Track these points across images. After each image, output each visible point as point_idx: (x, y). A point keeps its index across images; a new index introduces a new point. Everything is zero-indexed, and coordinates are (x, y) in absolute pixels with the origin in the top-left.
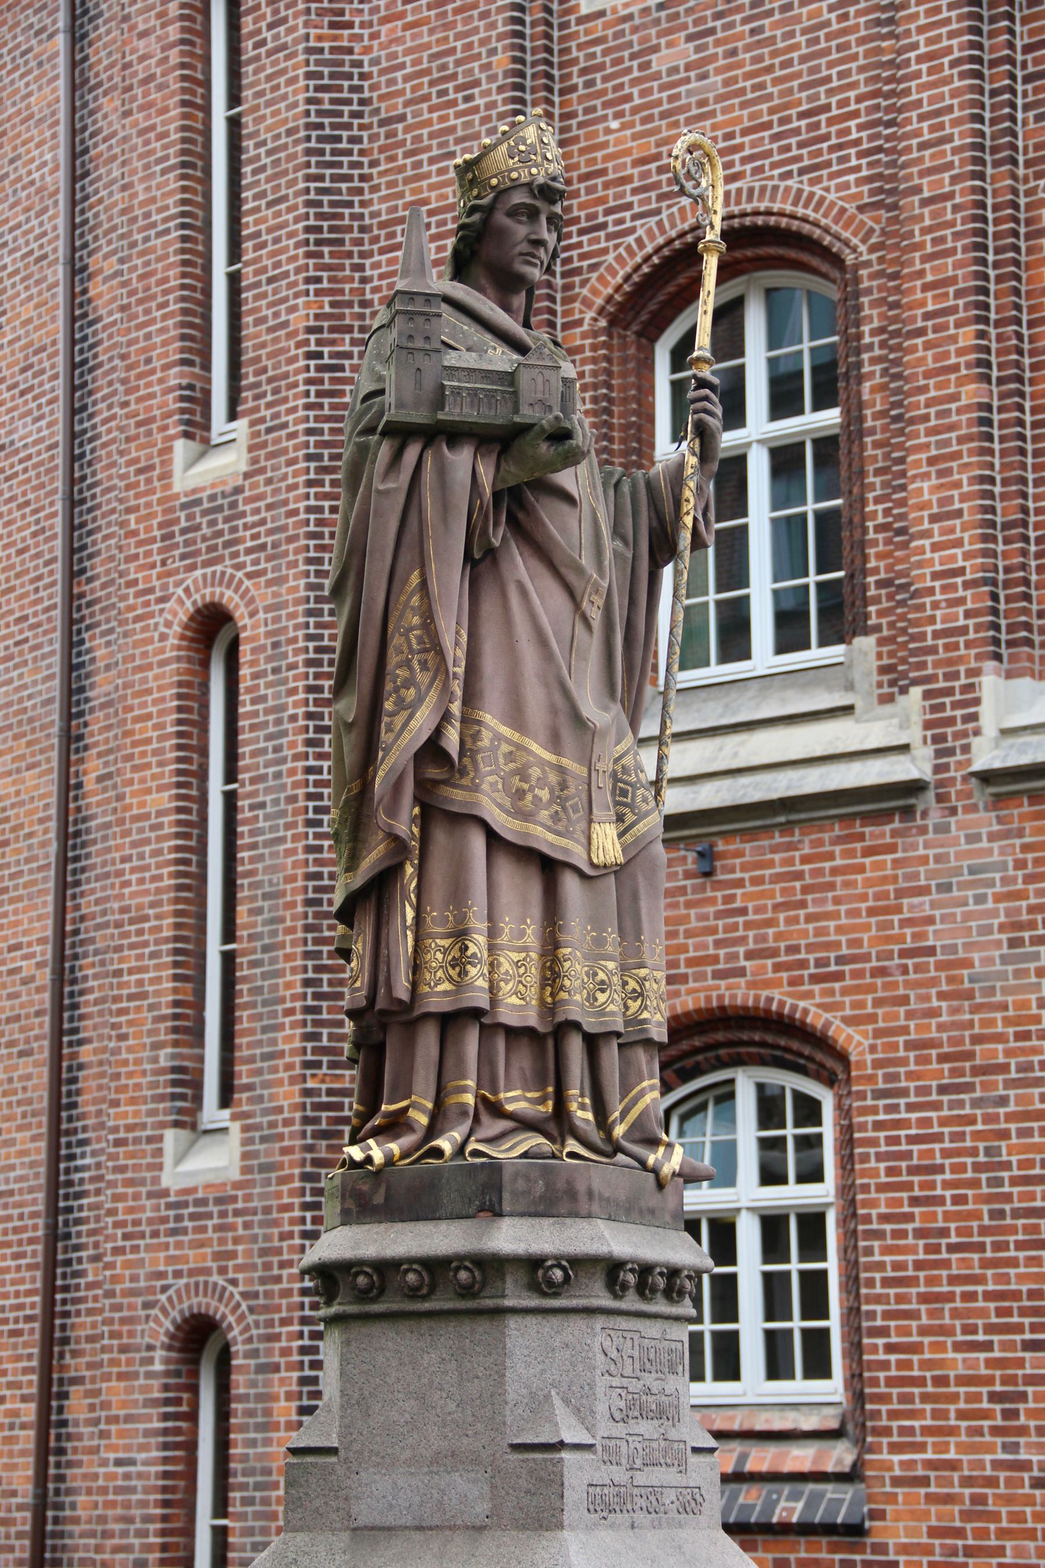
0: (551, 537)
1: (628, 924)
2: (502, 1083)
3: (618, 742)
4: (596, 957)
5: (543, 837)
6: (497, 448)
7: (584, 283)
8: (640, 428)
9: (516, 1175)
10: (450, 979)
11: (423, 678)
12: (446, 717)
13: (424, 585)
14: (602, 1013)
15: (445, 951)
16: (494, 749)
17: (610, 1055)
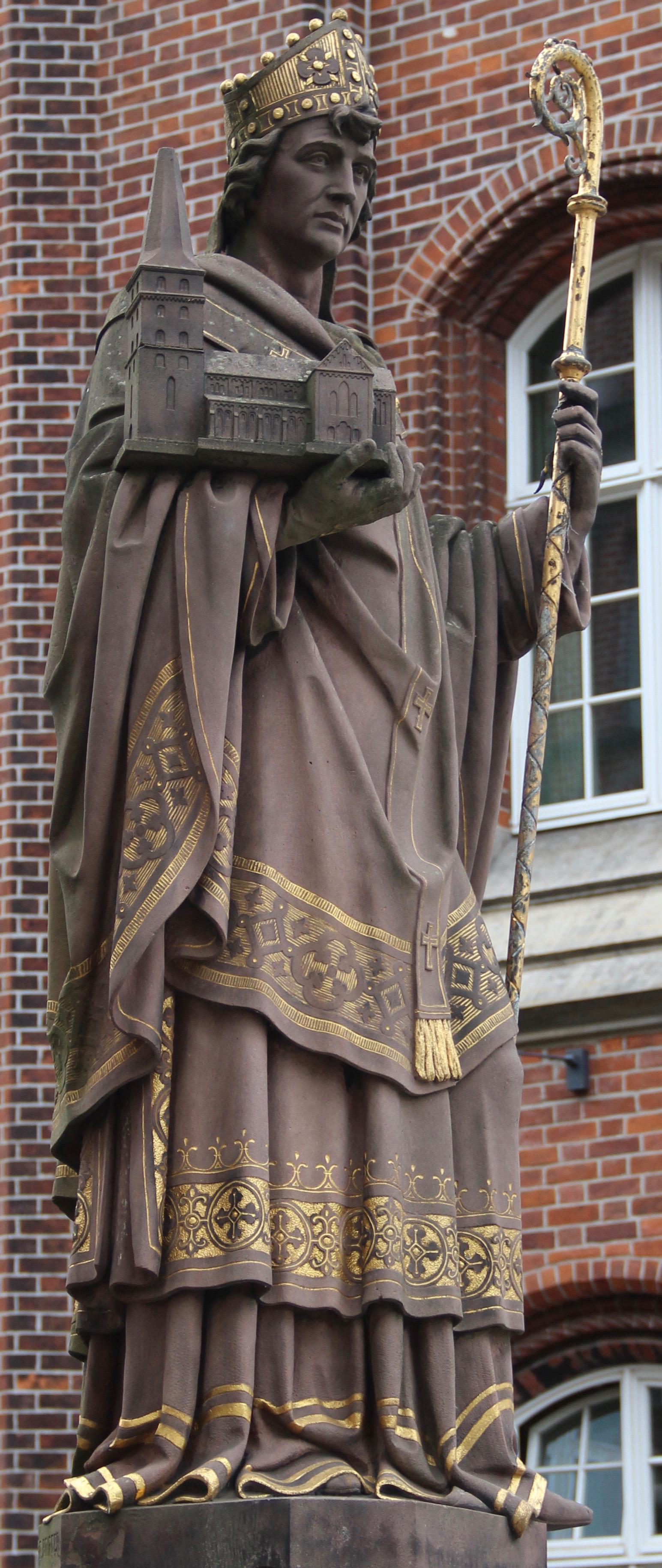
0: (358, 616)
1: (468, 1162)
2: (289, 1388)
3: (454, 906)
4: (422, 1208)
5: (348, 1040)
6: (284, 489)
7: (406, 256)
8: (485, 461)
9: (310, 1518)
10: (216, 1241)
11: (176, 814)
12: (211, 870)
13: (179, 683)
14: (431, 1289)
15: (209, 1202)
16: (278, 915)
17: (444, 1349)
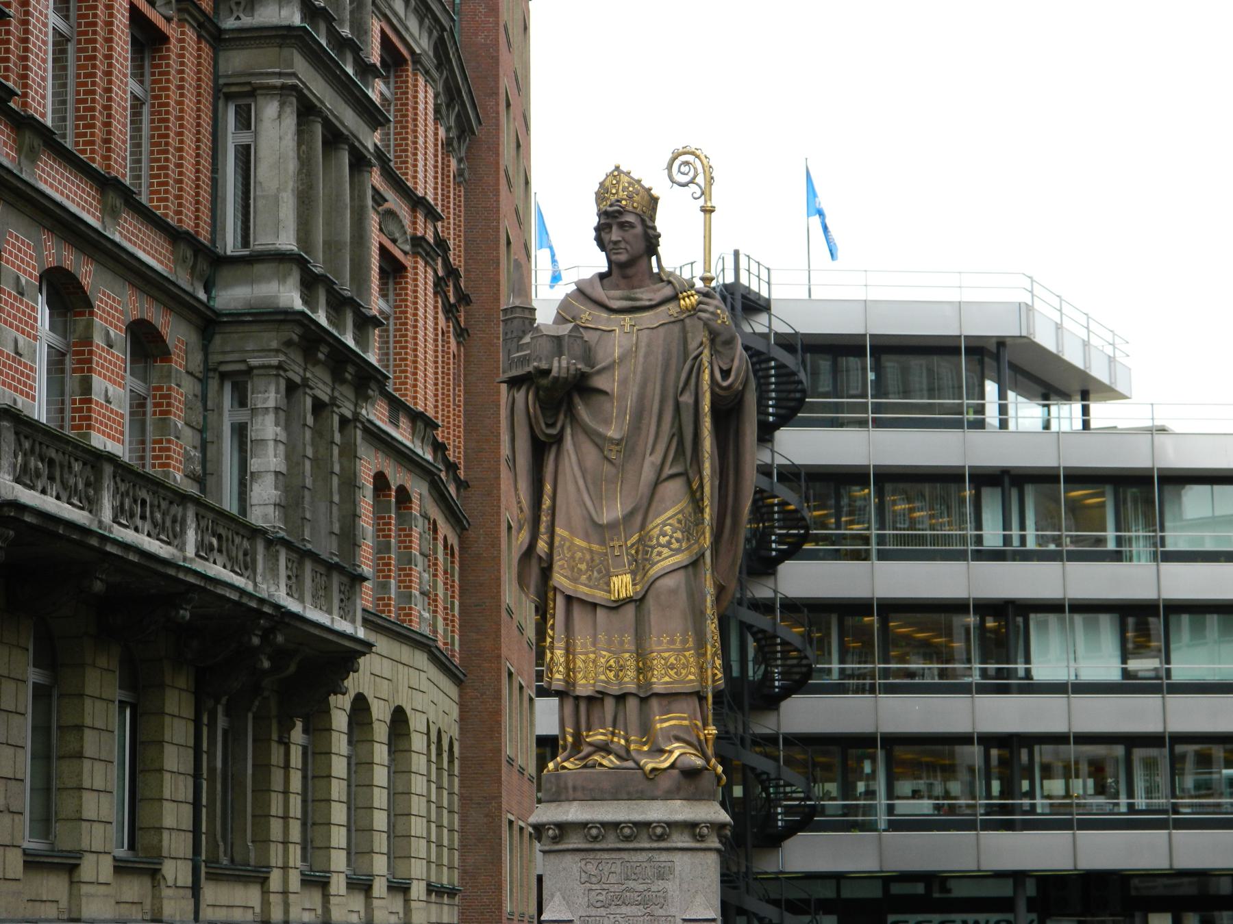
5: (583, 591)
16: (562, 546)
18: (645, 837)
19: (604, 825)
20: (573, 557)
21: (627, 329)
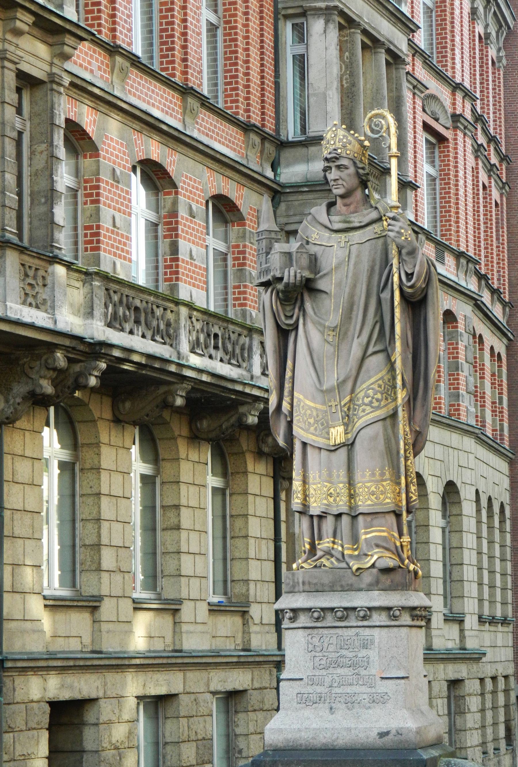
18: (353, 618)
19: (323, 609)
20: (305, 414)
21: (342, 245)
